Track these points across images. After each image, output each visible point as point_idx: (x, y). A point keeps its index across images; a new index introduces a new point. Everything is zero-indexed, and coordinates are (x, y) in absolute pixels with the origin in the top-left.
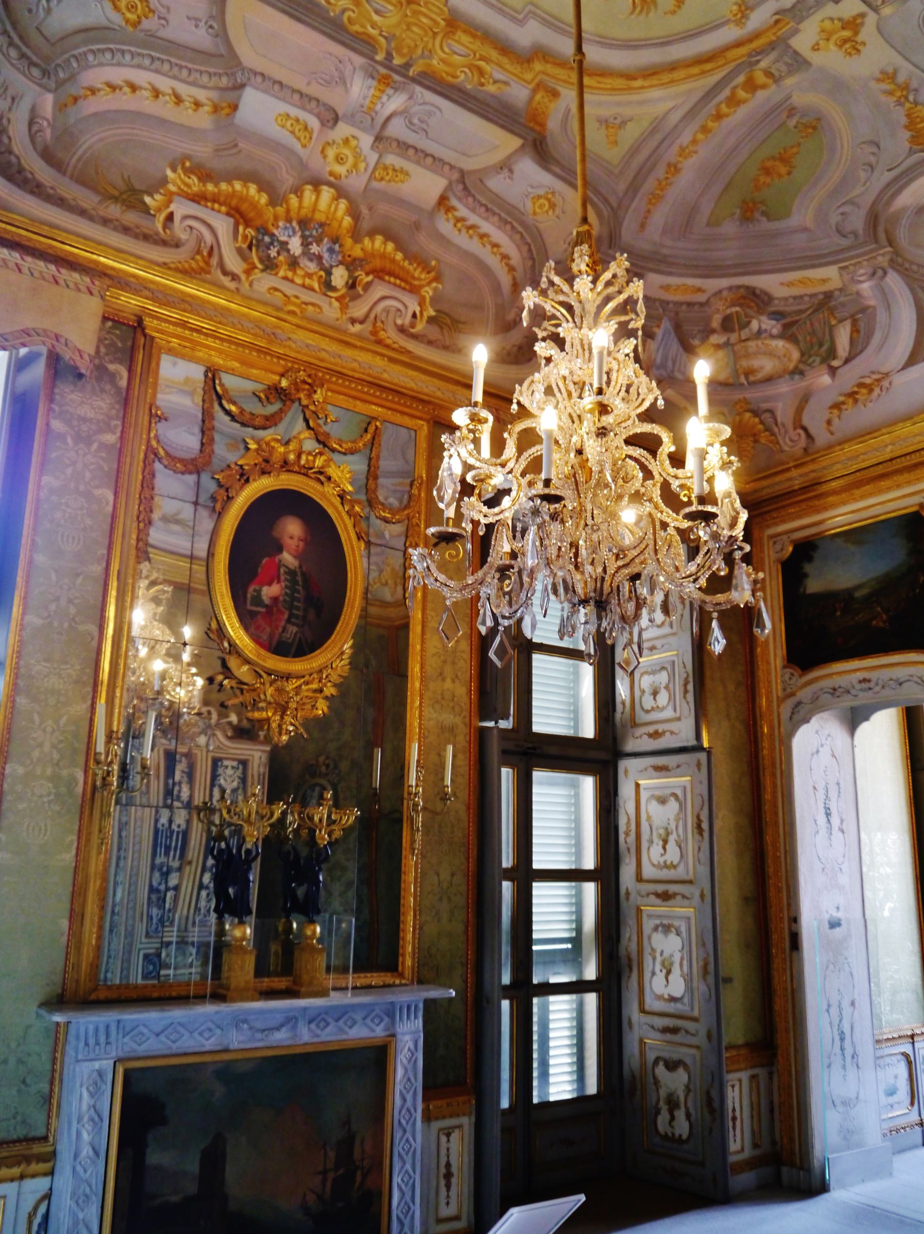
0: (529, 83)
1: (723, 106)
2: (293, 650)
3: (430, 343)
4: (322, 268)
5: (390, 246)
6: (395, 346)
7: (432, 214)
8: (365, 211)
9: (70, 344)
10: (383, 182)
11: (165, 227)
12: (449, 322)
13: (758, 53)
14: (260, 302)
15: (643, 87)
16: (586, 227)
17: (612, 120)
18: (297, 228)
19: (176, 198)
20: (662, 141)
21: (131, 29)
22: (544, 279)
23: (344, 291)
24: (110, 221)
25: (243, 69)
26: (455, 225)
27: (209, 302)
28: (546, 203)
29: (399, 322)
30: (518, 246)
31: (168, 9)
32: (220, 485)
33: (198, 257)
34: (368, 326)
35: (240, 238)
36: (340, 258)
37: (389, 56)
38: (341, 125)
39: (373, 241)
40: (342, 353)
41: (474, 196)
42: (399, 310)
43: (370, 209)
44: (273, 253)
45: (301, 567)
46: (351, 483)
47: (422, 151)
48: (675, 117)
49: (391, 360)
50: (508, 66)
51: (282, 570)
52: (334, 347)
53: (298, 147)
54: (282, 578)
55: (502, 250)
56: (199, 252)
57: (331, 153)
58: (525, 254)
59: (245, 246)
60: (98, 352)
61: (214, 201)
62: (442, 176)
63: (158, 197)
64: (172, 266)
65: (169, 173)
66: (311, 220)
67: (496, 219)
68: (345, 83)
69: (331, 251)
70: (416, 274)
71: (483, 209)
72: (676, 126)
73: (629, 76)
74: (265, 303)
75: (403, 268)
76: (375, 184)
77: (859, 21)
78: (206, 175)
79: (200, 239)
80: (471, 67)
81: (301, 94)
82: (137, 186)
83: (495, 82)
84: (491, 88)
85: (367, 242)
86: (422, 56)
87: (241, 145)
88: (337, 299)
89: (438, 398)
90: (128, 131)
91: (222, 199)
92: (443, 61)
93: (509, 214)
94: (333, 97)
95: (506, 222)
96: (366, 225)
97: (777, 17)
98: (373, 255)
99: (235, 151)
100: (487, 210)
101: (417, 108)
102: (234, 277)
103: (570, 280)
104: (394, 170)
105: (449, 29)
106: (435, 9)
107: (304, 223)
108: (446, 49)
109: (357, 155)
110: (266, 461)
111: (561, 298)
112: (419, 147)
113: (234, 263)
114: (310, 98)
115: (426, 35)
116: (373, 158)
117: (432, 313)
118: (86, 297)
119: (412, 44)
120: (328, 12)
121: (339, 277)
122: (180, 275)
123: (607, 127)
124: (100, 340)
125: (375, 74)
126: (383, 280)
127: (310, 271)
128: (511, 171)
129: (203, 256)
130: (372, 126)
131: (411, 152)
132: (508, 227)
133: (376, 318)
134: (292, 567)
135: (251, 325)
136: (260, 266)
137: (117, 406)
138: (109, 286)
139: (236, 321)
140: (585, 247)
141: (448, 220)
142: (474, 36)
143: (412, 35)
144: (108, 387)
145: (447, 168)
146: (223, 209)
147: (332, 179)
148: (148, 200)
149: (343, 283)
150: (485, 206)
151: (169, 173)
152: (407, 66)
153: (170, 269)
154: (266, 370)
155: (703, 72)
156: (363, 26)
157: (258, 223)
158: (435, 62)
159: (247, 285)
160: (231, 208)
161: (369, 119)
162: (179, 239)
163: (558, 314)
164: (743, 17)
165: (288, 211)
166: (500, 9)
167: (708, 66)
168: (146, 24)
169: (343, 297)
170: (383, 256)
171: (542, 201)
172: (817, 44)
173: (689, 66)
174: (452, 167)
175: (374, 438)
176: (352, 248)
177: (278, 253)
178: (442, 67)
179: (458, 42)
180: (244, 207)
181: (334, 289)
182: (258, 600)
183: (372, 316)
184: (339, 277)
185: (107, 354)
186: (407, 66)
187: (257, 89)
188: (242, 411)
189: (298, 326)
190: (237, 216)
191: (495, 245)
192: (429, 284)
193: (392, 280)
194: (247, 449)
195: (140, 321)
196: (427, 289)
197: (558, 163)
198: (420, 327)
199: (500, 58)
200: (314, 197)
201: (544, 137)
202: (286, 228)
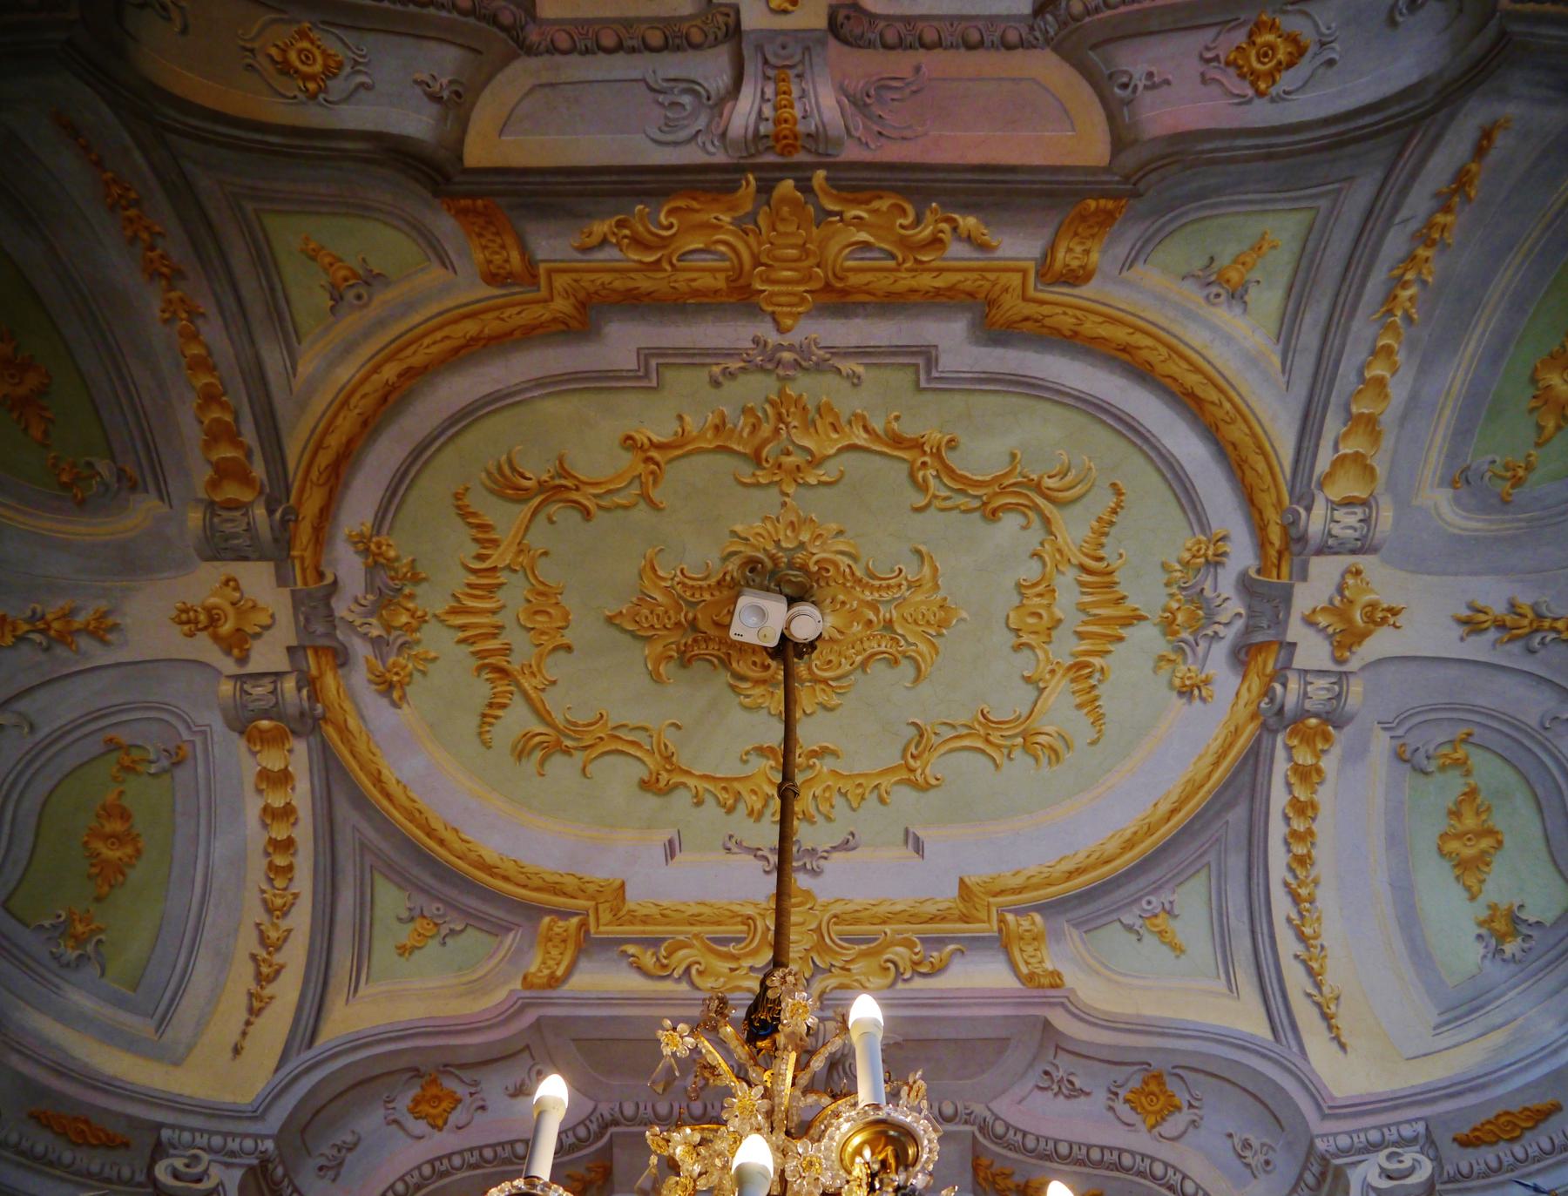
0: (550, 273)
1: (228, 418)
13: (284, 522)
15: (376, 369)
17: (363, 290)
20: (239, 300)
21: (1264, 18)
25: (1048, 41)
31: (1204, 80)
37: (805, 187)
38: (822, 23)
47: (633, 50)
48: (273, 358)
50: (607, 278)
68: (854, 103)
72: (252, 342)
73: (416, 378)
77: (236, 652)
80: (664, 243)
81: (923, 45)
83: (604, 242)
84: (601, 227)
86: (753, 217)
92: (717, 228)
94: (865, 65)
97: (329, 579)
101: (701, 123)
105: (742, 282)
106: (783, 299)
108: (722, 248)
114: (901, 45)
115: (769, 252)
119: (781, 227)
120: (943, 205)
123: (355, 275)
125: (810, 144)
128: (435, 98)
130: (760, 48)
131: (655, 38)
142: (696, 293)
143: (792, 241)
145: (563, 41)
152: (765, 188)
155: (319, 446)
156: (875, 212)
158: (726, 218)
161: (772, 60)
164: (367, 550)
166: (694, 355)
167: (324, 459)
168: (1240, 37)
172: (237, 588)
173: (350, 442)
174: (553, 49)
178: (709, 217)
179: (713, 271)
186: (765, 188)
187: (1009, 17)
199: (631, 284)
201: (436, 194)
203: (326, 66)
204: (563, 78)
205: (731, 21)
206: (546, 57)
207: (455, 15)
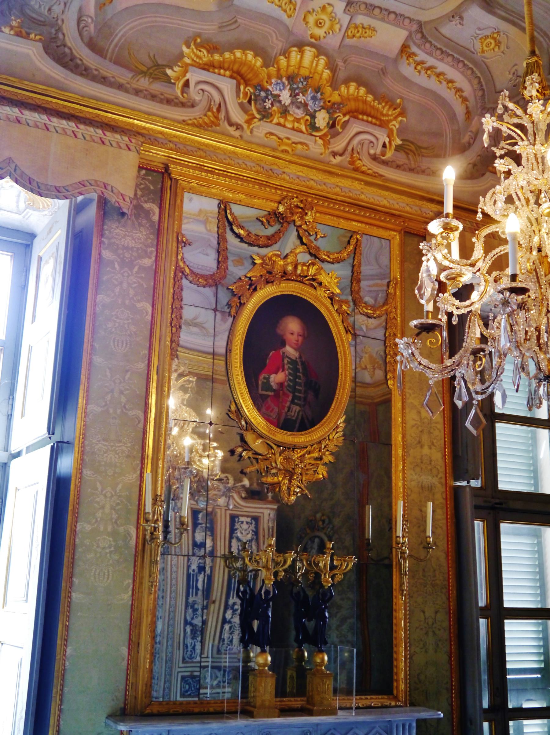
2: (297, 425)
3: (398, 167)
4: (308, 113)
5: (362, 90)
6: (370, 172)
7: (395, 61)
8: (340, 64)
9: (115, 191)
10: (355, 39)
11: (183, 92)
12: (413, 147)
14: (258, 145)
16: (535, 59)
18: (286, 83)
19: (190, 68)
22: (500, 106)
23: (326, 130)
24: (141, 91)
26: (416, 68)
27: (219, 148)
28: (493, 41)
29: (372, 152)
30: (470, 81)
32: (234, 294)
33: (209, 113)
34: (347, 157)
35: (241, 95)
36: (322, 104)
39: (348, 88)
40: (327, 181)
41: (430, 42)
42: (372, 142)
43: (344, 63)
44: (268, 105)
45: (300, 357)
46: (338, 286)
47: (386, 10)
49: (367, 183)
51: (286, 362)
52: (320, 177)
53: (284, 17)
54: (286, 367)
55: (456, 85)
56: (210, 109)
57: (311, 19)
58: (476, 87)
59: (246, 101)
60: (136, 194)
61: (220, 68)
62: (405, 29)
63: (176, 69)
64: (190, 122)
65: (185, 49)
66: (298, 75)
67: (450, 59)
69: (314, 98)
70: (385, 112)
71: (438, 52)
74: (264, 146)
75: (373, 107)
76: (348, 41)
78: (213, 48)
79: (210, 100)
82: (160, 62)
85: (343, 89)
87: (239, 20)
88: (320, 137)
89: (407, 212)
90: (154, 19)
91: (226, 65)
93: (461, 54)
95: (459, 61)
96: (342, 75)
98: (348, 99)
99: (237, 25)
100: (442, 52)
102: (238, 127)
103: (523, 103)
104: (363, 28)
107: (291, 78)
109: (333, 19)
110: (270, 273)
111: (516, 120)
112: (383, 7)
113: (238, 116)
116: (346, 19)
117: (399, 142)
118: (125, 153)
121: (322, 119)
122: (196, 129)
124: (137, 185)
126: (358, 118)
127: (298, 117)
128: (461, 18)
129: (213, 112)
131: (377, 11)
132: (461, 65)
133: (353, 149)
134: (294, 358)
135: (252, 164)
136: (258, 116)
137: (152, 236)
138: (143, 143)
139: (241, 162)
140: (535, 76)
141: (409, 64)
144: (144, 222)
145: (407, 21)
146: (228, 73)
147: (313, 40)
148: (169, 72)
149: (325, 124)
150: (440, 49)
151: (185, 49)
153: (188, 124)
154: (267, 199)
157: (255, 82)
159: (248, 132)
160: (233, 72)
162: (194, 100)
163: (514, 134)
165: (279, 70)
169: (325, 135)
170: (356, 99)
171: (488, 40)
174: (411, 20)
175: (355, 249)
176: (331, 95)
177: (272, 104)
180: (244, 70)
181: (318, 129)
182: (267, 386)
183: (350, 148)
184: (322, 119)
185: (142, 196)
188: (249, 233)
189: (291, 162)
190: (239, 78)
191: (451, 81)
192: (396, 118)
193: (365, 118)
194: (254, 264)
195: (167, 168)
196: (394, 122)
197: (502, 6)
198: (389, 154)
200: (299, 57)
202: (277, 83)
203: (485, 39)
204: (415, 9)
205: (348, 8)
206: (416, 19)
207: (433, 42)
